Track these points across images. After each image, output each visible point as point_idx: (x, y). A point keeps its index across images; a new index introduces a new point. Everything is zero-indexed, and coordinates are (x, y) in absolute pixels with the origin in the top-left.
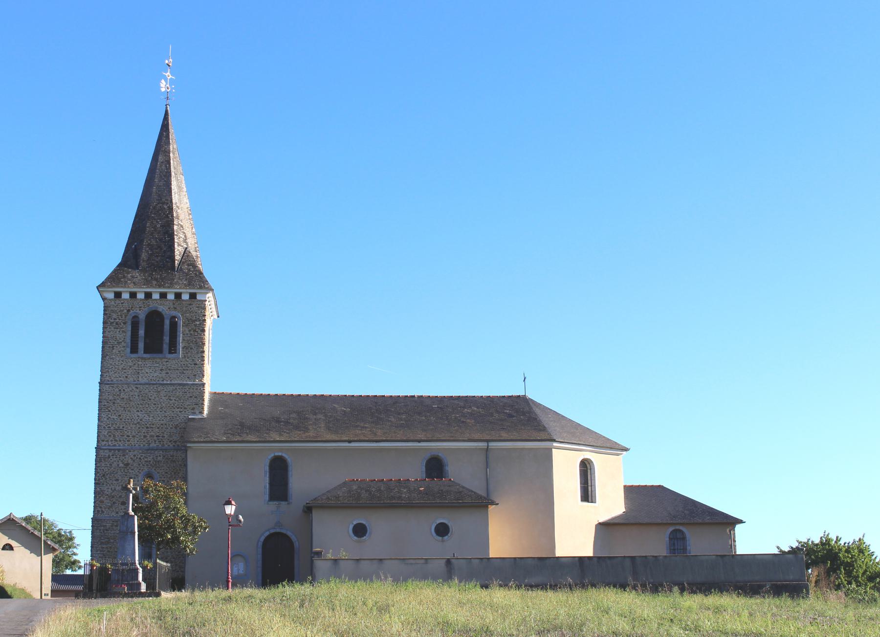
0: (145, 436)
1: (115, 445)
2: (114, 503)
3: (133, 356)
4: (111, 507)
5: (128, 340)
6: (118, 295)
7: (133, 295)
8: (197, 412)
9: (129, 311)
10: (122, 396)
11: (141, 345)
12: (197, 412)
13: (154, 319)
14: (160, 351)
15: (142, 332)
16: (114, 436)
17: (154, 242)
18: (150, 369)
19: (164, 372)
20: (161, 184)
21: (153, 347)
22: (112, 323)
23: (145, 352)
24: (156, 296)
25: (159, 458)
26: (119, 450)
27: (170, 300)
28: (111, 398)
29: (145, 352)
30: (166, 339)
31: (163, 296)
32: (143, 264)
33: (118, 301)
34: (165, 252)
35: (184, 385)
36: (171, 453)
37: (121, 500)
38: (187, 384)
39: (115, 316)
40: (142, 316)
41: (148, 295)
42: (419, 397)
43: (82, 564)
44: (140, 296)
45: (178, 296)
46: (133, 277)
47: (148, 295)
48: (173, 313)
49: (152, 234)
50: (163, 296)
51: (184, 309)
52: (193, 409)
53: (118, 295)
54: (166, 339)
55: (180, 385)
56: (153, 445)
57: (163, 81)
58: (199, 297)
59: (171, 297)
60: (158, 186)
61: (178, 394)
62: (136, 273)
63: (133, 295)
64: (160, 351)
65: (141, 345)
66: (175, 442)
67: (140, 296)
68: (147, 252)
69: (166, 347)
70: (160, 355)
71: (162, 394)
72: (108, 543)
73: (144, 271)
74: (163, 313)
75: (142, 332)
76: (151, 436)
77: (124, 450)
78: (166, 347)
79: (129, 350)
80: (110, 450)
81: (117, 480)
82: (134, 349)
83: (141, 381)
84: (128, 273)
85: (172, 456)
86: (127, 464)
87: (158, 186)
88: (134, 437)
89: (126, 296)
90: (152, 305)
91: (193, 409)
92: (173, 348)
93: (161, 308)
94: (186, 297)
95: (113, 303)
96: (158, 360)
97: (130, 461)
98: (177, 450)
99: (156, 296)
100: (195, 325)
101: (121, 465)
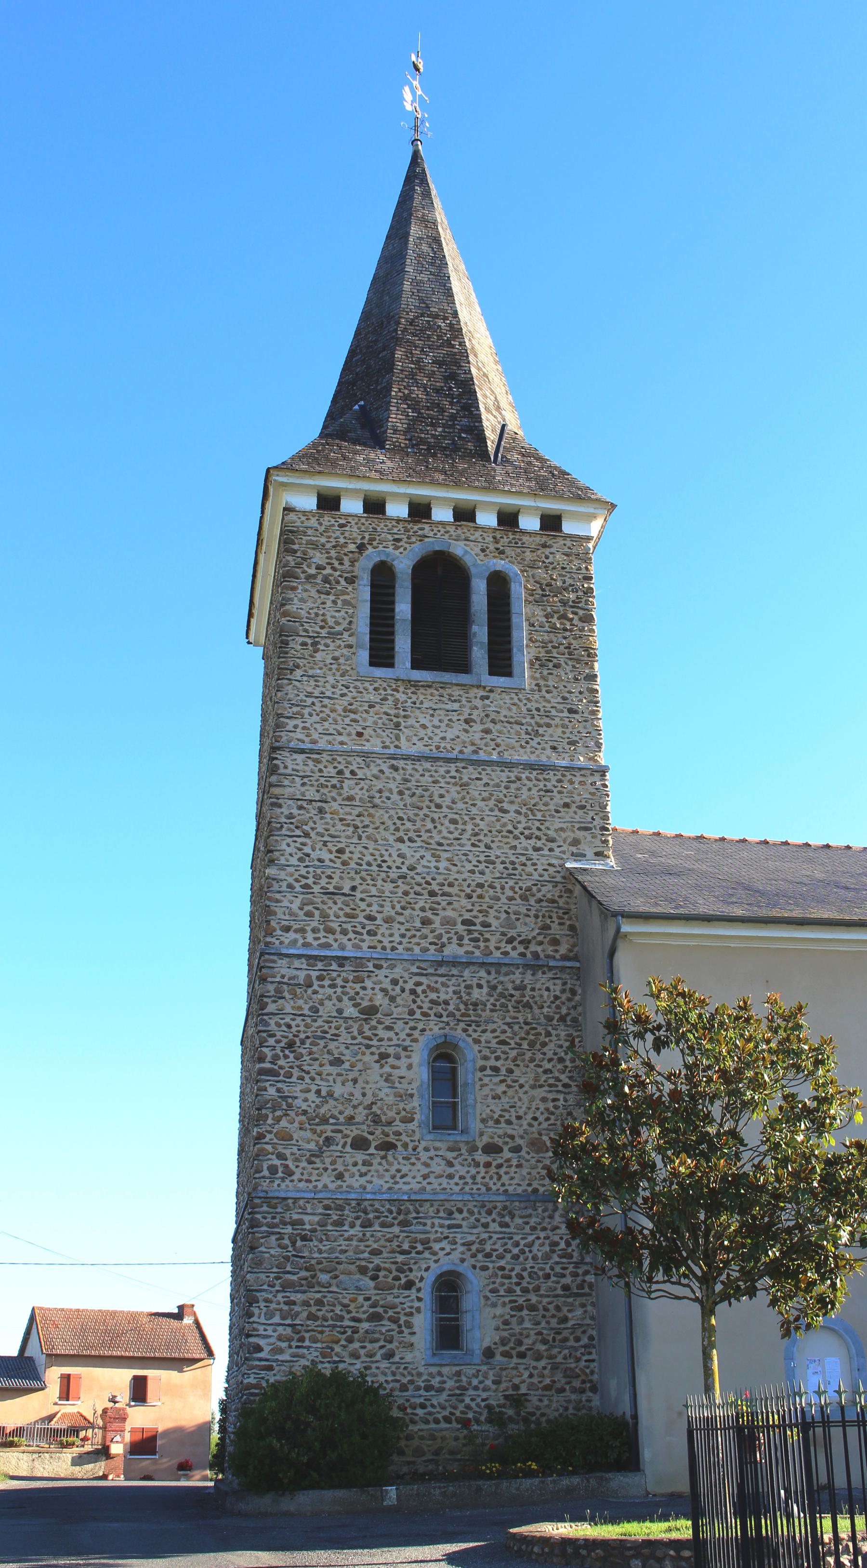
0: (425, 922)
1: (327, 946)
2: (328, 1141)
3: (379, 672)
4: (319, 1154)
5: (363, 626)
6: (329, 502)
7: (375, 507)
8: (590, 853)
9: (361, 548)
10: (346, 792)
11: (403, 644)
12: (590, 853)
13: (440, 576)
14: (463, 666)
15: (403, 608)
16: (324, 916)
17: (418, 393)
18: (437, 715)
19: (478, 727)
20: (424, 277)
21: (441, 649)
22: (309, 577)
23: (416, 665)
24: (442, 514)
25: (476, 994)
26: (341, 961)
27: (483, 529)
28: (311, 793)
29: (416, 665)
30: (480, 632)
31: (464, 515)
32: (394, 439)
33: (327, 520)
34: (453, 417)
35: (543, 768)
36: (517, 977)
37: (353, 1132)
38: (554, 768)
39: (319, 558)
40: (404, 564)
41: (420, 511)
42: (228, 1381)
43: (129, 1410)
44: (397, 510)
45: (508, 520)
46: (368, 461)
47: (420, 511)
48: (500, 564)
49: (412, 375)
50: (464, 515)
51: (528, 555)
52: (576, 842)
53: (329, 502)
54: (480, 632)
55: (531, 767)
56: (452, 950)
57: (407, 89)
58: (568, 527)
59: (487, 519)
60: (416, 283)
61: (525, 794)
62: (378, 456)
63: (375, 507)
64: (463, 666)
65: (403, 644)
66: (526, 943)
67: (397, 510)
68: (404, 413)
69: (479, 655)
70: (463, 678)
71: (476, 789)
72: (311, 1284)
73: (398, 450)
74: (468, 560)
75: (403, 608)
76: (446, 922)
77: (359, 962)
78: (479, 655)
79: (364, 655)
80: (312, 959)
81: (337, 1062)
82: (382, 655)
83: (406, 748)
84: (356, 453)
85: (521, 988)
86: (370, 1011)
87: (416, 283)
88: (388, 920)
89: (352, 506)
90: (435, 541)
91: (576, 842)
92: (501, 662)
93: (458, 549)
94: (530, 523)
95: (313, 522)
96: (456, 692)
97: (380, 999)
98: (535, 968)
99: (442, 514)
100: (564, 603)
101: (350, 1011)
